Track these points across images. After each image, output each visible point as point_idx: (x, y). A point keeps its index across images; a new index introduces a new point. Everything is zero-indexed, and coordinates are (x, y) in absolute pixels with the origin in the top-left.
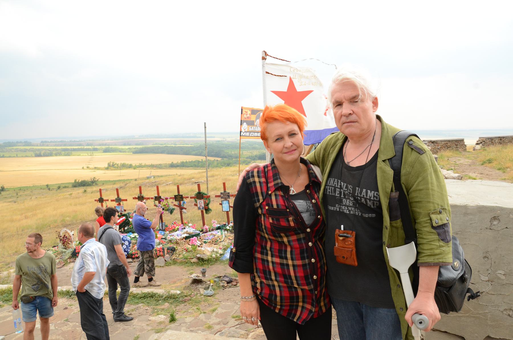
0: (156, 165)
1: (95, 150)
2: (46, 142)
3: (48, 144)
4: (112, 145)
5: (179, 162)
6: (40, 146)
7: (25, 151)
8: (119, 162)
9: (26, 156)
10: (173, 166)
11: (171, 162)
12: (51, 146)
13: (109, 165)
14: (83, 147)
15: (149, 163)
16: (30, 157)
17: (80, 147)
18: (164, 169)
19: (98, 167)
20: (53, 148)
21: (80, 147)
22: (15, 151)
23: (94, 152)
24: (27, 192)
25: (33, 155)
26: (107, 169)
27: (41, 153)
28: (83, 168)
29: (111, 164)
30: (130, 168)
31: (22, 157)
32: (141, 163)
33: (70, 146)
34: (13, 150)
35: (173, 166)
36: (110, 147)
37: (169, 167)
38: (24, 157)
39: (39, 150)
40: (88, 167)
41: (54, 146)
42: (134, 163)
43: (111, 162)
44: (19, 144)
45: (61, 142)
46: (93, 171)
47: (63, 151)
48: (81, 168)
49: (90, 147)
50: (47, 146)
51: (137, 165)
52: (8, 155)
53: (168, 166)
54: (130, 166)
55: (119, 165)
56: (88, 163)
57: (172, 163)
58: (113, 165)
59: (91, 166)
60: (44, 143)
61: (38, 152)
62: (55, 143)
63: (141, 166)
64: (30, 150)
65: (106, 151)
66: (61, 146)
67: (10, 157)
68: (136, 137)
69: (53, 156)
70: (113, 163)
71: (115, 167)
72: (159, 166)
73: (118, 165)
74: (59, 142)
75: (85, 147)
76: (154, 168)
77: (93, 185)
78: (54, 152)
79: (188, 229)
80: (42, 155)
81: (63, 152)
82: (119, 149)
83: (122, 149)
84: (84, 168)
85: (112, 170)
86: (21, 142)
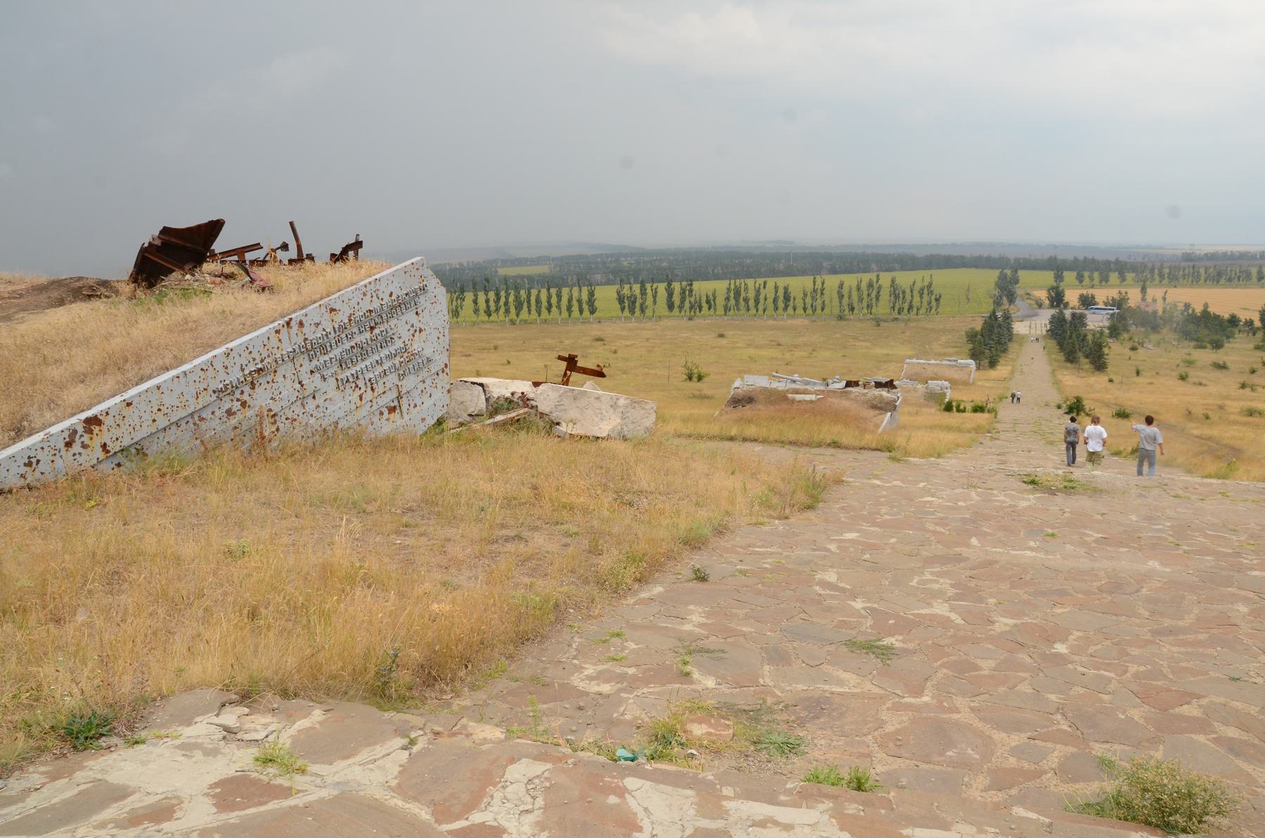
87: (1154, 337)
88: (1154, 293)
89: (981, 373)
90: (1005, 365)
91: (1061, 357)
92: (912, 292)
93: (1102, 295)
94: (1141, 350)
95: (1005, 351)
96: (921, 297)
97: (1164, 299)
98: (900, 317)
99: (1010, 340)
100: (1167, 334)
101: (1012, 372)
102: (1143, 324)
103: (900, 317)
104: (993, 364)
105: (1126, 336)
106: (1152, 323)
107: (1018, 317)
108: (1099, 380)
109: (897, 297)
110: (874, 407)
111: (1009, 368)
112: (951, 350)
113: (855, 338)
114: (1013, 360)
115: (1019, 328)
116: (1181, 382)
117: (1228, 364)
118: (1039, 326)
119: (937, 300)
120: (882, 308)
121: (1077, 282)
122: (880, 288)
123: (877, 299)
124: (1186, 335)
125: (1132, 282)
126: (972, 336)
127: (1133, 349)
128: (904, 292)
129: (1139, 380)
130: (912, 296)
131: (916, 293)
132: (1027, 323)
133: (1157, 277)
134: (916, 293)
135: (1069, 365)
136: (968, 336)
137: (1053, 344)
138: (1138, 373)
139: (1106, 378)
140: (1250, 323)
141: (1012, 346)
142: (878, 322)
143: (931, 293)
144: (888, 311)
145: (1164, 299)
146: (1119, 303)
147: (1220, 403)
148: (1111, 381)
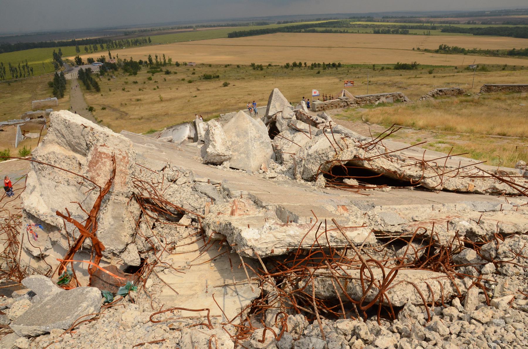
0: (493, 51)
1: (434, 28)
2: (387, 17)
3: (388, 19)
4: (454, 23)
5: (524, 48)
6: (381, 22)
7: (366, 26)
8: (451, 45)
9: (366, 33)
10: (512, 53)
11: (512, 49)
12: (391, 22)
13: (440, 47)
14: (422, 24)
15: (484, 48)
16: (369, 33)
17: (419, 24)
18: (500, 57)
19: (429, 49)
20: (392, 25)
21: (419, 24)
22: (358, 27)
23: (430, 31)
24: (357, 70)
25: (373, 32)
26: (437, 52)
27: (379, 30)
28: (413, 49)
29: (443, 47)
30: (461, 52)
31: (363, 33)
32: (475, 48)
33: (409, 22)
34: (356, 26)
35: (512, 53)
36: (451, 25)
37: (508, 55)
38: (364, 33)
39: (379, 26)
40: (418, 49)
41: (394, 22)
42: (467, 47)
43: (443, 45)
44: (362, 19)
45: (402, 17)
46: (422, 53)
47: (400, 28)
48: (412, 49)
49: (429, 25)
50: (388, 22)
51: (470, 49)
52: (351, 31)
53: (506, 53)
54: (462, 51)
55: (451, 49)
56: (420, 44)
57: (514, 49)
58: (445, 48)
59: (421, 48)
60: (385, 19)
61: (377, 29)
62: (396, 19)
63: (474, 52)
64: (370, 26)
65: (445, 30)
66: (400, 22)
67: (352, 33)
68: (486, 13)
69: (391, 34)
70: (445, 46)
71: (446, 51)
72: (496, 52)
73: (449, 48)
74: (400, 18)
75: (425, 24)
76: (487, 55)
77: (413, 69)
78: (392, 30)
79: (107, 169)
80: (380, 32)
81: (400, 30)
82: (460, 28)
83: (463, 29)
84: (415, 49)
85: (442, 53)
86: (364, 17)
87: (116, 73)
88: (114, 53)
89: (59, 100)
90: (66, 95)
91: (85, 88)
92: (19, 68)
93: (96, 56)
94: (112, 80)
95: (65, 89)
96: (24, 70)
97: (117, 57)
98: (17, 79)
99: (66, 83)
100: (120, 71)
101: (70, 98)
102: (111, 68)
103: (17, 79)
104: (62, 96)
105: (106, 74)
106: (113, 67)
107: (66, 72)
108: (98, 96)
109: (13, 71)
110: (40, 123)
111: (68, 96)
112: (44, 92)
113: (3, 93)
114: (69, 92)
115: (68, 76)
116: (123, 91)
117: (138, 81)
118: (75, 75)
119: (32, 70)
120: (8, 76)
121: (86, 52)
122: (4, 68)
123: (5, 73)
124: (126, 70)
125: (106, 49)
126: (51, 85)
127: (109, 80)
128: (16, 69)
129: (111, 93)
130: (20, 70)
131: (21, 69)
132: (70, 74)
133: (115, 46)
134: (21, 69)
135: (88, 91)
136: (49, 85)
137: (81, 82)
138: (110, 90)
139: (100, 94)
140: (146, 62)
141: (67, 86)
142: (9, 83)
143: (28, 67)
144: (11, 77)
145: (117, 57)
146: (102, 60)
147: (129, 98)
148: (102, 95)
